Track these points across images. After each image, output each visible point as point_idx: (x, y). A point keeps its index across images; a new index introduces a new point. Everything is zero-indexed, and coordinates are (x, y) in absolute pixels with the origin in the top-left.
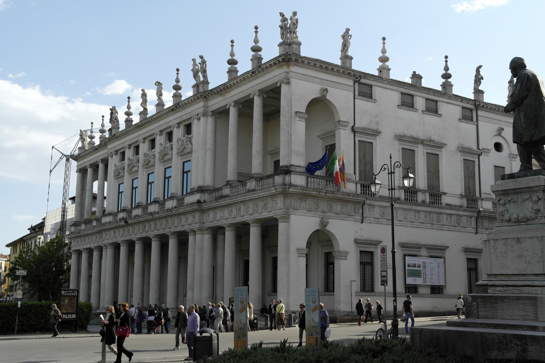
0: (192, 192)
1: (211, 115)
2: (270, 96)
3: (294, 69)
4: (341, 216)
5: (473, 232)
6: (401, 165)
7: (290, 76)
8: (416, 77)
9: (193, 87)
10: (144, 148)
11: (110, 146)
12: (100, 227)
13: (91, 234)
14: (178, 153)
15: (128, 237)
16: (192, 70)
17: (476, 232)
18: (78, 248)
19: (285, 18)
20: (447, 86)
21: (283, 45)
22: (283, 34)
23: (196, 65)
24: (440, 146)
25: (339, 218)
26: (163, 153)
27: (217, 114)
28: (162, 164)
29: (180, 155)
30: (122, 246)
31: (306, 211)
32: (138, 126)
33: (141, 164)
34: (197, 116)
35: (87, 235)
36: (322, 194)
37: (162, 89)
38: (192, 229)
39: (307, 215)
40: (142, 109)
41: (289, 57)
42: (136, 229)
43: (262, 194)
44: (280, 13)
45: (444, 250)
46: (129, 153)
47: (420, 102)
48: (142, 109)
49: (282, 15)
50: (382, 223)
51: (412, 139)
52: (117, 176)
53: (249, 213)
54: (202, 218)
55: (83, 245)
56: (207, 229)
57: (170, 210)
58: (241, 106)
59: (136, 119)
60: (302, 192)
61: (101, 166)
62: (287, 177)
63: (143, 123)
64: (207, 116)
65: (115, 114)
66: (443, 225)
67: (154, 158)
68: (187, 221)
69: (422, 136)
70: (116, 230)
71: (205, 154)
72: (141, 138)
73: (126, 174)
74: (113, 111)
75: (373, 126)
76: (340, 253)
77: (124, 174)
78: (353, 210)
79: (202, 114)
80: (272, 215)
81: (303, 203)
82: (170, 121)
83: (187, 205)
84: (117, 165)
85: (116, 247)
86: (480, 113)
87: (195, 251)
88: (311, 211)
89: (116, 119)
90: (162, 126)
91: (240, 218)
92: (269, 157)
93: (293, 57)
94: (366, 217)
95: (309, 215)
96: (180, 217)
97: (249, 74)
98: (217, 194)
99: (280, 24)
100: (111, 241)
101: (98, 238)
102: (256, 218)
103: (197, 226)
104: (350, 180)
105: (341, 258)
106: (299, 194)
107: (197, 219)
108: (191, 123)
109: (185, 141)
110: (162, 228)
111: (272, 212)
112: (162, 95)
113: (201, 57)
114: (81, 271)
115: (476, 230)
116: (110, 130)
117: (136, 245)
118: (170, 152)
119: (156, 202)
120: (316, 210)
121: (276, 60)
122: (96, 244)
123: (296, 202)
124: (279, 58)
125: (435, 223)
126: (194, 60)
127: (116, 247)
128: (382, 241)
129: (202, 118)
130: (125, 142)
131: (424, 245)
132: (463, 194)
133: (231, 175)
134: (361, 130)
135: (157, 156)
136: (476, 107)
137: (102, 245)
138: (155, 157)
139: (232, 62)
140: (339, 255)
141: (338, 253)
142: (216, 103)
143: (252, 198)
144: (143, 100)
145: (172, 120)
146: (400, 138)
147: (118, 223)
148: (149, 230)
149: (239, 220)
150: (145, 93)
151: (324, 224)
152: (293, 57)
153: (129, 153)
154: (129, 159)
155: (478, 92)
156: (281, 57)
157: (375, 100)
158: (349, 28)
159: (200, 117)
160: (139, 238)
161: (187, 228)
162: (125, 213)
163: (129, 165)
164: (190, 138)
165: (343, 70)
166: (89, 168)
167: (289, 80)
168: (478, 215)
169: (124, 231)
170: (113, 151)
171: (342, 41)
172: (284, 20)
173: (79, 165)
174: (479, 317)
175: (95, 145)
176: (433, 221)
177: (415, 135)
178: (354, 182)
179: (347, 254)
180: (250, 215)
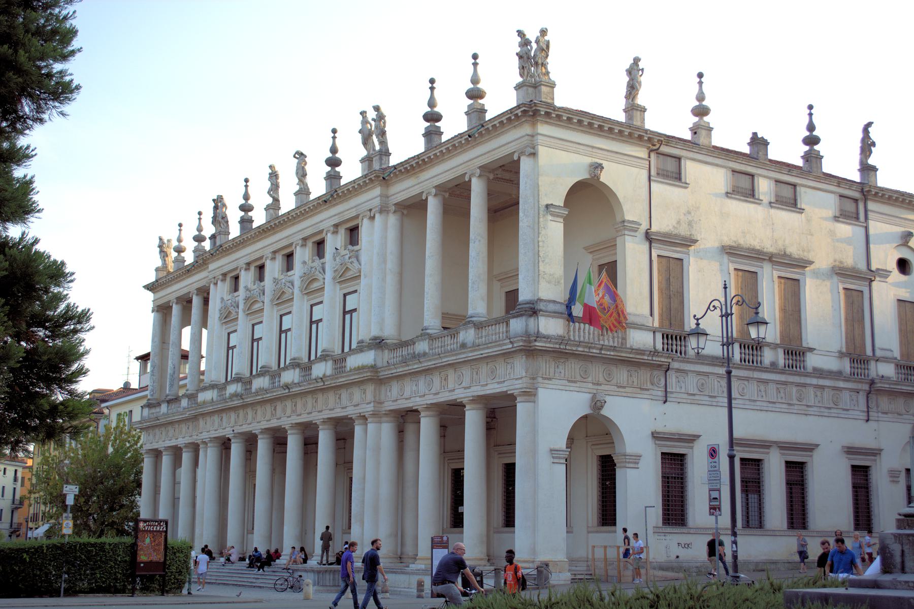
0: (362, 347)
1: (395, 212)
2: (499, 176)
3: (543, 129)
4: (627, 390)
5: (861, 417)
6: (743, 301)
7: (535, 142)
8: (758, 143)
9: (363, 161)
10: (273, 269)
11: (212, 266)
12: (194, 410)
13: (180, 422)
14: (334, 279)
15: (244, 426)
16: (360, 132)
17: (866, 418)
18: (155, 446)
19: (527, 39)
20: (812, 158)
21: (525, 88)
22: (523, 67)
23: (367, 122)
24: (802, 264)
25: (624, 394)
26: (308, 279)
27: (404, 209)
28: (306, 297)
29: (339, 282)
30: (233, 443)
31: (565, 382)
32: (263, 230)
33: (267, 299)
34: (369, 212)
35: (171, 423)
36: (594, 351)
37: (306, 164)
38: (360, 413)
39: (567, 388)
40: (270, 200)
41: (534, 108)
42: (259, 412)
43: (486, 351)
44: (518, 31)
45: (811, 450)
46: (247, 278)
47: (764, 186)
48: (270, 200)
49: (520, 33)
50: (700, 402)
51: (752, 253)
52: (225, 318)
53: (464, 385)
54: (378, 394)
55: (164, 441)
56: (387, 413)
57: (321, 379)
58: (447, 195)
59: (259, 218)
60: (560, 348)
61: (196, 302)
62: (532, 321)
63: (271, 224)
64: (388, 212)
65: (222, 208)
66: (808, 406)
67: (291, 286)
68: (351, 399)
69: (769, 248)
70: (224, 415)
71: (384, 280)
72: (268, 252)
73: (241, 315)
74: (219, 203)
75: (683, 231)
76: (627, 457)
77: (238, 315)
78: (648, 380)
79: (377, 209)
80: (505, 389)
81: (561, 367)
82: (321, 221)
83: (351, 370)
84: (225, 299)
85: (225, 444)
86: (871, 206)
87: (365, 453)
88: (575, 382)
89: (224, 218)
90: (305, 231)
91: (447, 394)
92: (497, 285)
93: (541, 109)
94: (672, 393)
95: (571, 389)
96: (339, 392)
97: (464, 138)
98: (405, 351)
99: (518, 50)
100: (214, 434)
101: (191, 428)
102: (476, 394)
103: (370, 408)
104: (644, 326)
105: (627, 465)
106: (553, 351)
107: (369, 396)
108: (358, 224)
109: (347, 257)
110: (307, 411)
111: (506, 384)
112: (306, 175)
113: (377, 108)
114: (160, 487)
115: (865, 414)
116: (213, 237)
117: (259, 441)
118: (320, 277)
119: (295, 364)
120: (584, 379)
121: (511, 113)
122: (188, 440)
123: (548, 366)
124: (517, 110)
125: (795, 402)
126: (363, 113)
127: (225, 444)
128: (700, 436)
129: (377, 216)
130: (240, 258)
131: (776, 443)
132: (844, 350)
133: (431, 320)
134: (662, 237)
135: (297, 283)
136: (864, 195)
137: (199, 442)
138: (293, 285)
139: (432, 117)
140: (624, 460)
141: (623, 457)
142: (403, 190)
143: (469, 358)
144: (272, 184)
145: (325, 220)
146: (731, 251)
147: (227, 402)
148: (282, 415)
149: (445, 397)
150: (276, 172)
151: (597, 405)
152: (541, 109)
153: (247, 278)
154: (247, 289)
155: (867, 169)
156: (520, 108)
157: (686, 183)
158: (640, 57)
159: (375, 215)
160: (265, 429)
161: (351, 412)
162: (240, 384)
163: (247, 299)
164: (357, 251)
165: (629, 131)
166: (175, 307)
167: (534, 148)
168: (870, 388)
169: (238, 416)
170: (218, 273)
171: (627, 79)
172: (525, 43)
173: (156, 300)
174: (907, 570)
175: (186, 264)
176: (792, 399)
177: (756, 244)
178: (650, 330)
179: (638, 458)
180: (465, 388)
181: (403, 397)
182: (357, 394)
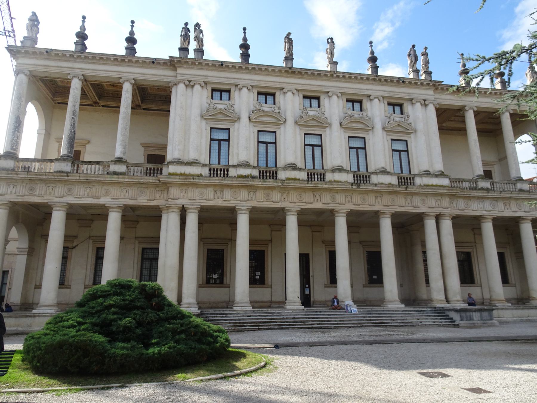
15: (264, 203)
90: (345, 89)
91: (511, 213)
130: (241, 79)
181: (470, 209)
182: (431, 202)
